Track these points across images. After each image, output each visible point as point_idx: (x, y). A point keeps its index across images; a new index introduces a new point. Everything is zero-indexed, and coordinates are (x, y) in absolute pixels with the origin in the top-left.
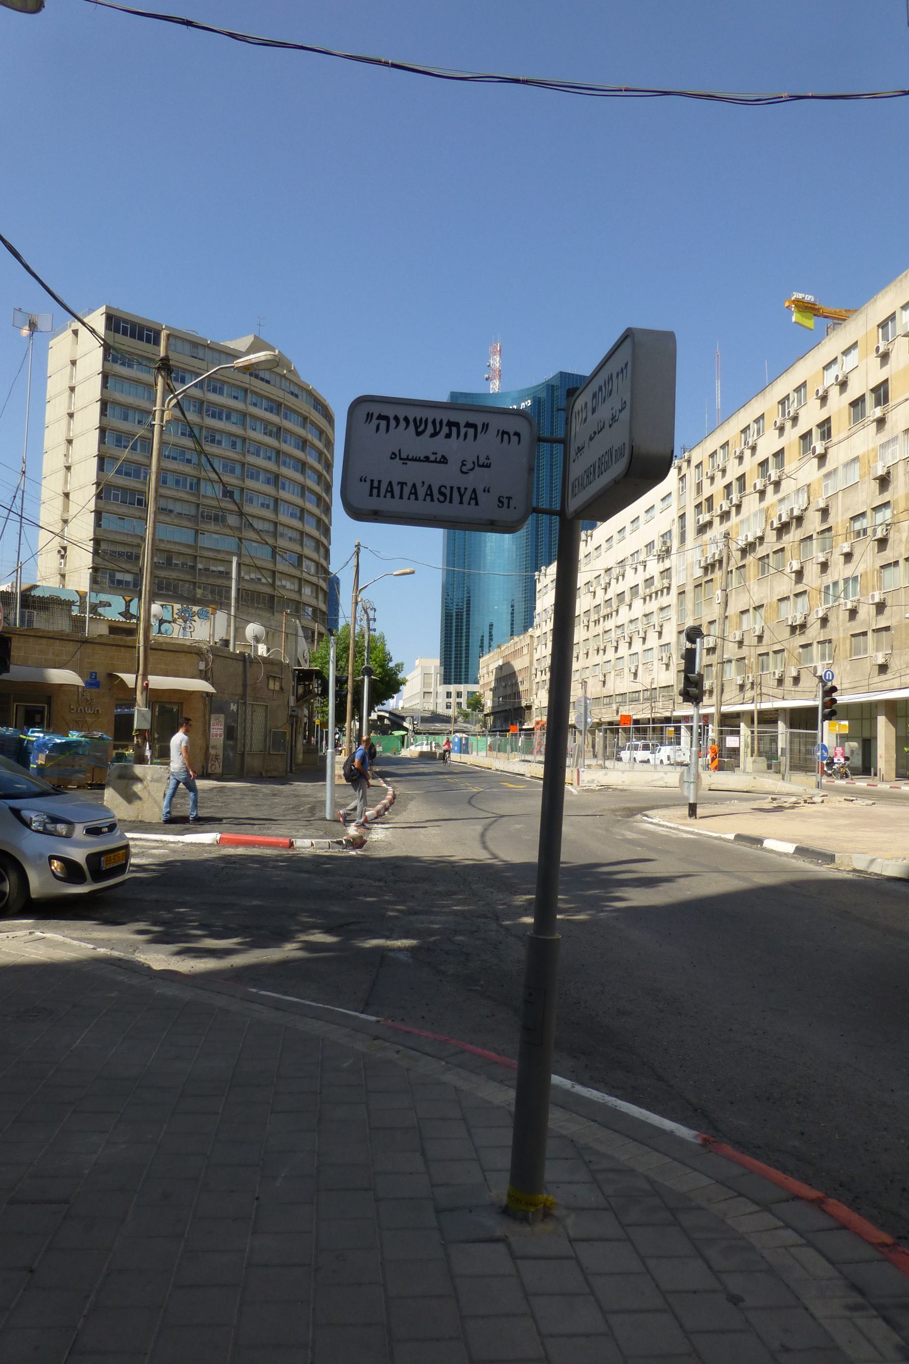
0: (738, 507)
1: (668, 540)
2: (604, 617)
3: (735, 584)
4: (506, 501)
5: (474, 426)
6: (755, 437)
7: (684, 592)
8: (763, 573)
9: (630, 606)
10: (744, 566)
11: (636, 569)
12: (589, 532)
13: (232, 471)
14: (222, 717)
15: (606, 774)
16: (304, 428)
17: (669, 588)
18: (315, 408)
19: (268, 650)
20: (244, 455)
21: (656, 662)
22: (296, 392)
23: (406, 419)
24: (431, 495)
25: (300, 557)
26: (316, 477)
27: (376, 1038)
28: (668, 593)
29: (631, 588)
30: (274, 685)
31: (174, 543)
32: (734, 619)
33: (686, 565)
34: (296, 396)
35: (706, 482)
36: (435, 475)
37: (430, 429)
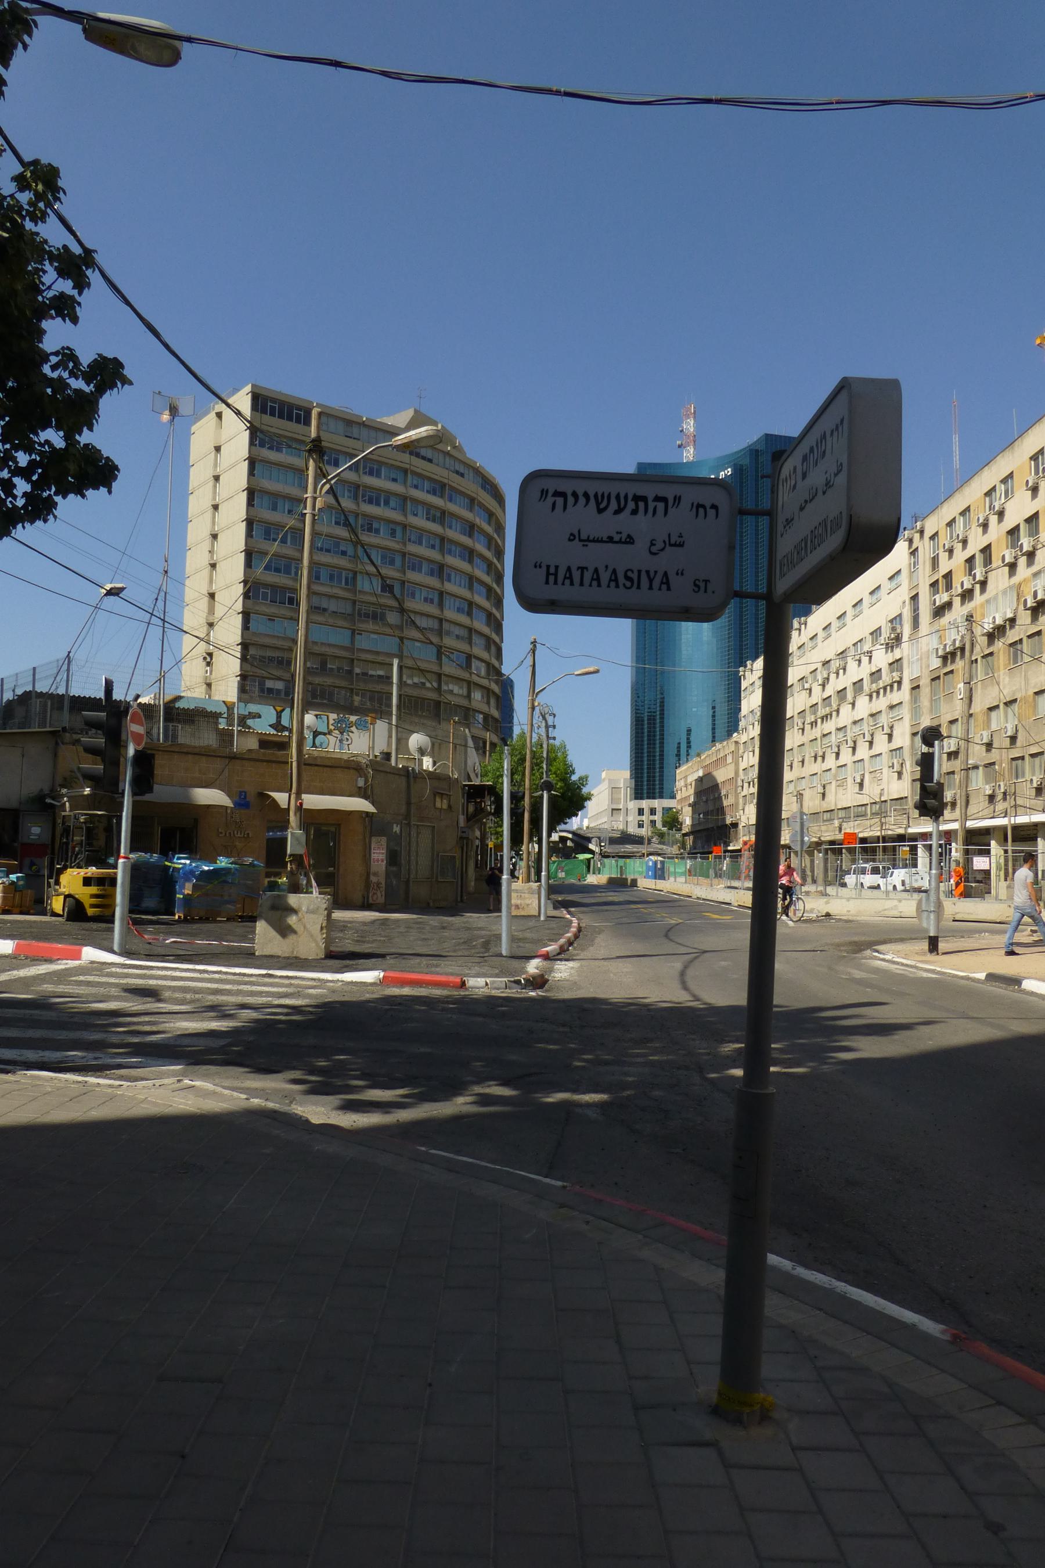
0: (983, 584)
1: (898, 626)
2: (822, 718)
3: (981, 676)
4: (702, 585)
5: (664, 500)
6: (1003, 501)
7: (918, 687)
8: (1015, 661)
9: (853, 704)
10: (991, 654)
11: (860, 661)
12: (803, 619)
13: (392, 562)
14: (384, 840)
15: (827, 903)
16: (471, 511)
17: (899, 683)
18: (483, 487)
19: (434, 763)
20: (405, 544)
21: (885, 770)
22: (462, 471)
23: (586, 495)
24: (616, 580)
25: (469, 657)
26: (485, 566)
27: (562, 1206)
28: (899, 688)
29: (854, 684)
30: (441, 804)
31: (330, 645)
32: (981, 718)
33: (920, 654)
34: (462, 475)
35: (943, 556)
36: (622, 558)
37: (614, 505)
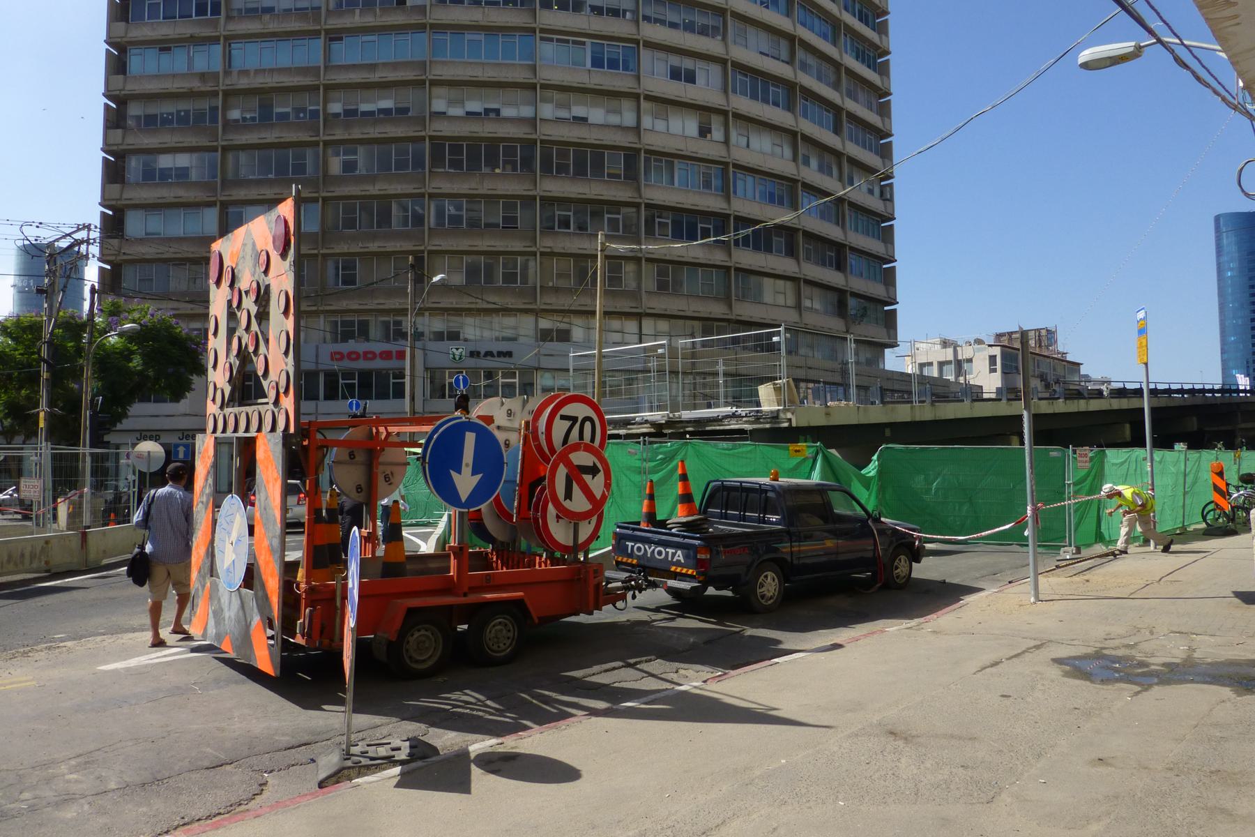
31: (272, 71)
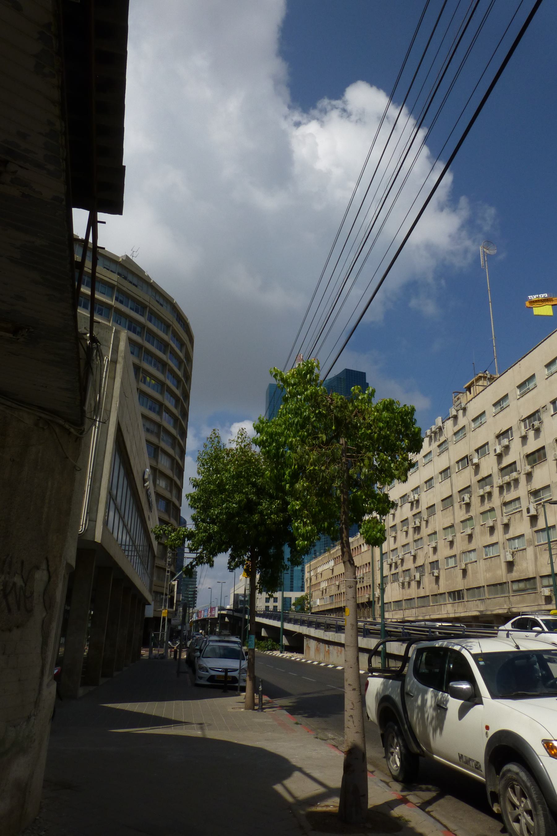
2: (501, 488)
22: (161, 301)
34: (162, 305)
